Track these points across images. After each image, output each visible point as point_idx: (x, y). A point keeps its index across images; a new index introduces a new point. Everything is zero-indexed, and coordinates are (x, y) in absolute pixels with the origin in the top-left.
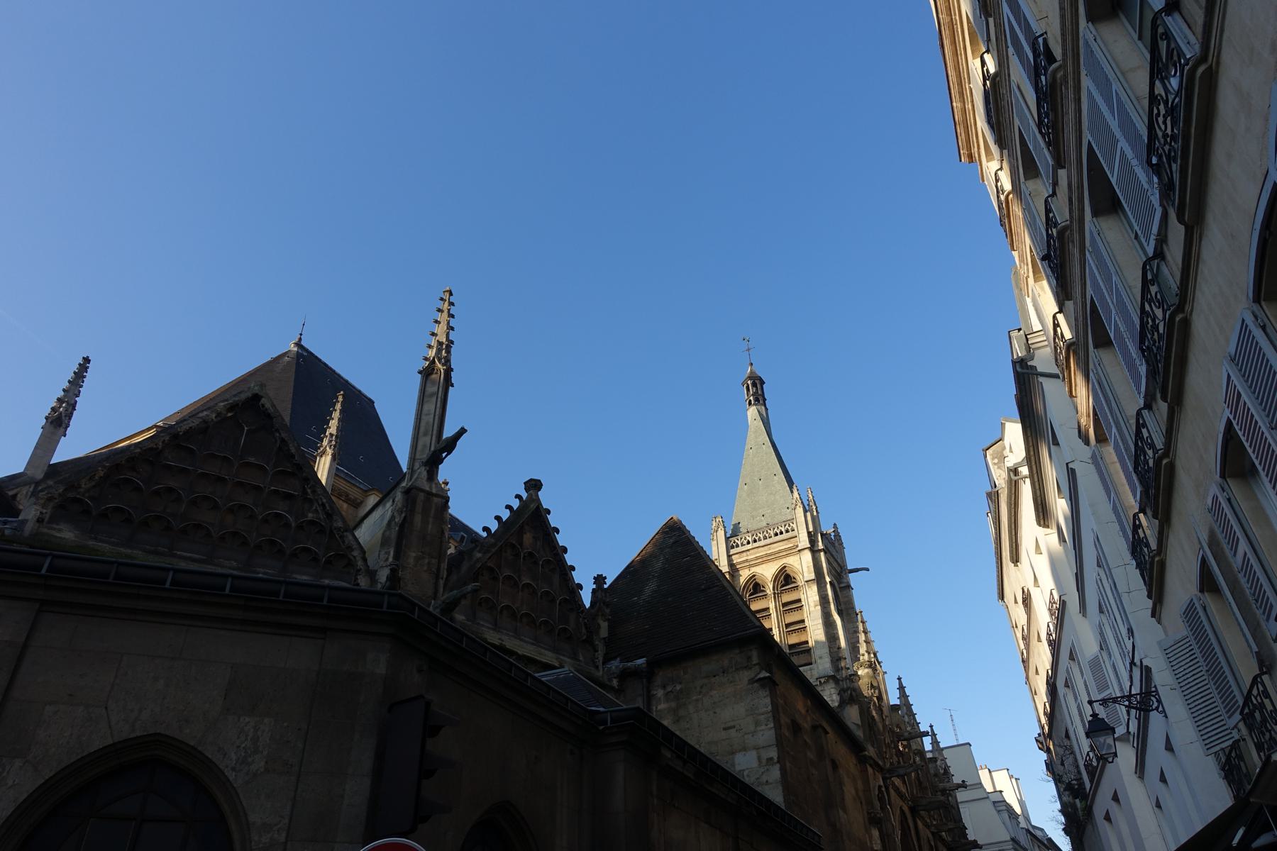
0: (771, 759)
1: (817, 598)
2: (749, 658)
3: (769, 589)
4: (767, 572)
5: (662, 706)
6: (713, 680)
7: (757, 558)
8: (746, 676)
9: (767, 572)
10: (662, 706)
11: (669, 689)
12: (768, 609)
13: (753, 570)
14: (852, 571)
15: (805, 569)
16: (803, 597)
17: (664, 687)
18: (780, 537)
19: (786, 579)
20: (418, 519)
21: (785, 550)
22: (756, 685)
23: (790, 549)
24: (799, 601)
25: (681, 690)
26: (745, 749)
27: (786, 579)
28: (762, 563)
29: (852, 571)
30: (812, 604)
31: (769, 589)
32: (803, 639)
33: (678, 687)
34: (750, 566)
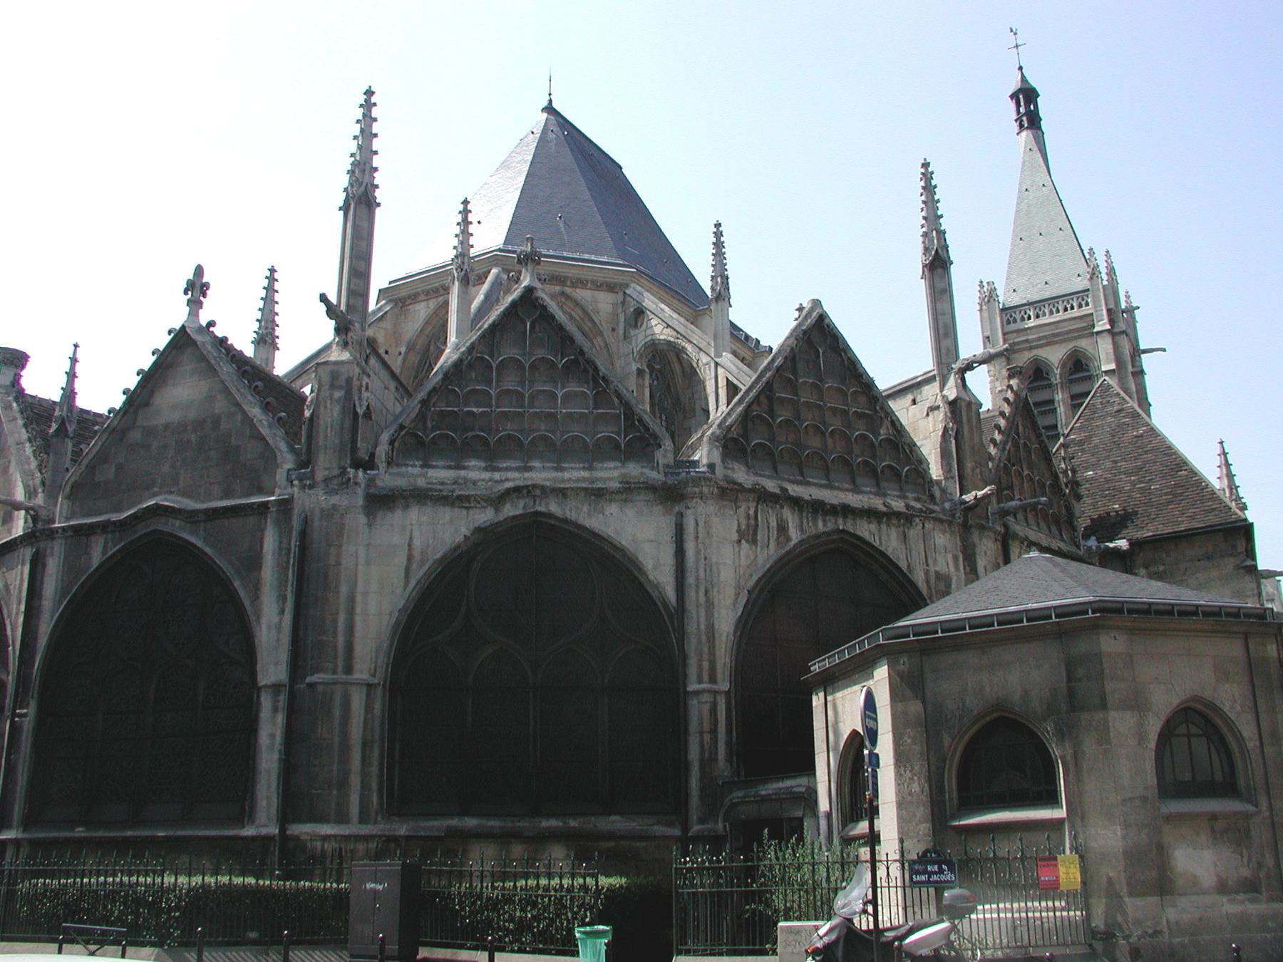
2: (1234, 547)
3: (1056, 375)
4: (1055, 356)
6: (1198, 564)
7: (1040, 339)
8: (1230, 563)
9: (1055, 356)
11: (1153, 569)
12: (1052, 401)
13: (1035, 352)
14: (1145, 351)
17: (1147, 568)
21: (1077, 330)
23: (1084, 329)
25: (1165, 572)
28: (1048, 344)
29: (1145, 351)
33: (1161, 568)
34: (1031, 348)
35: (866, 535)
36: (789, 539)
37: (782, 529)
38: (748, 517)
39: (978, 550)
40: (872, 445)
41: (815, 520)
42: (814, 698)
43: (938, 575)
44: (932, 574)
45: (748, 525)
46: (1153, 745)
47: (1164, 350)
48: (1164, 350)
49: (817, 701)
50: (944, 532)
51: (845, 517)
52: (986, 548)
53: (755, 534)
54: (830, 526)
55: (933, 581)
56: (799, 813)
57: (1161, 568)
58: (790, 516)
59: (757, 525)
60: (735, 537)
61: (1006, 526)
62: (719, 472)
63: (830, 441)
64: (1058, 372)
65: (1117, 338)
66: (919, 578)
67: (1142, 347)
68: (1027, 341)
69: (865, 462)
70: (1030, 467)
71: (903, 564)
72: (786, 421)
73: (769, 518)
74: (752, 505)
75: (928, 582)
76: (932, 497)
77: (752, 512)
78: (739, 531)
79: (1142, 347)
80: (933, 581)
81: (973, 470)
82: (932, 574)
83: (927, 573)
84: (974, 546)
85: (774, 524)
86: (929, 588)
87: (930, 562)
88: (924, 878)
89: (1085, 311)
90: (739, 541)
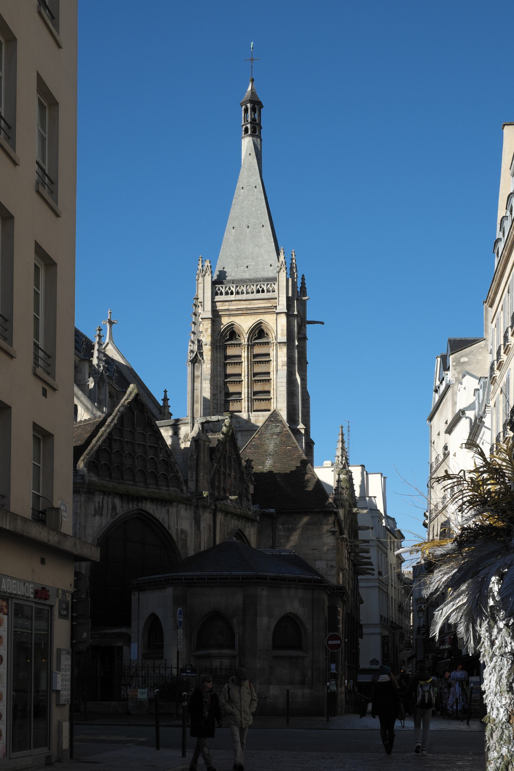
0: (333, 566)
1: (285, 359)
4: (245, 324)
5: (281, 533)
7: (238, 310)
9: (245, 324)
10: (281, 533)
12: (240, 356)
15: (279, 332)
16: (273, 353)
17: (283, 525)
18: (261, 295)
19: (259, 332)
20: (202, 455)
21: (264, 308)
22: (330, 533)
24: (268, 355)
26: (321, 560)
27: (259, 332)
30: (280, 364)
31: (244, 340)
32: (266, 389)
33: (291, 526)
35: (151, 511)
36: (116, 514)
37: (114, 508)
38: (99, 503)
39: (201, 519)
40: (156, 463)
41: (128, 503)
42: (133, 596)
43: (183, 532)
44: (179, 530)
45: (99, 507)
46: (272, 630)
47: (322, 323)
48: (322, 323)
49: (134, 597)
50: (186, 510)
51: (142, 502)
52: (206, 517)
53: (102, 511)
54: (135, 507)
55: (179, 534)
56: (120, 644)
57: (291, 526)
58: (117, 502)
59: (103, 507)
60: (93, 513)
61: (216, 505)
62: (87, 479)
63: (136, 461)
64: (246, 336)
65: (291, 318)
66: (173, 532)
67: (308, 319)
68: (228, 310)
69: (152, 472)
70: (230, 469)
71: (166, 526)
72: (117, 451)
73: (108, 501)
74: (101, 497)
75: (177, 535)
76: (182, 490)
77: (101, 501)
78: (95, 510)
79: (308, 319)
80: (179, 534)
81: (204, 476)
82: (179, 530)
83: (177, 529)
84: (200, 517)
85: (110, 506)
86: (177, 537)
87: (179, 524)
88: (185, 674)
89: (270, 295)
90: (94, 515)
